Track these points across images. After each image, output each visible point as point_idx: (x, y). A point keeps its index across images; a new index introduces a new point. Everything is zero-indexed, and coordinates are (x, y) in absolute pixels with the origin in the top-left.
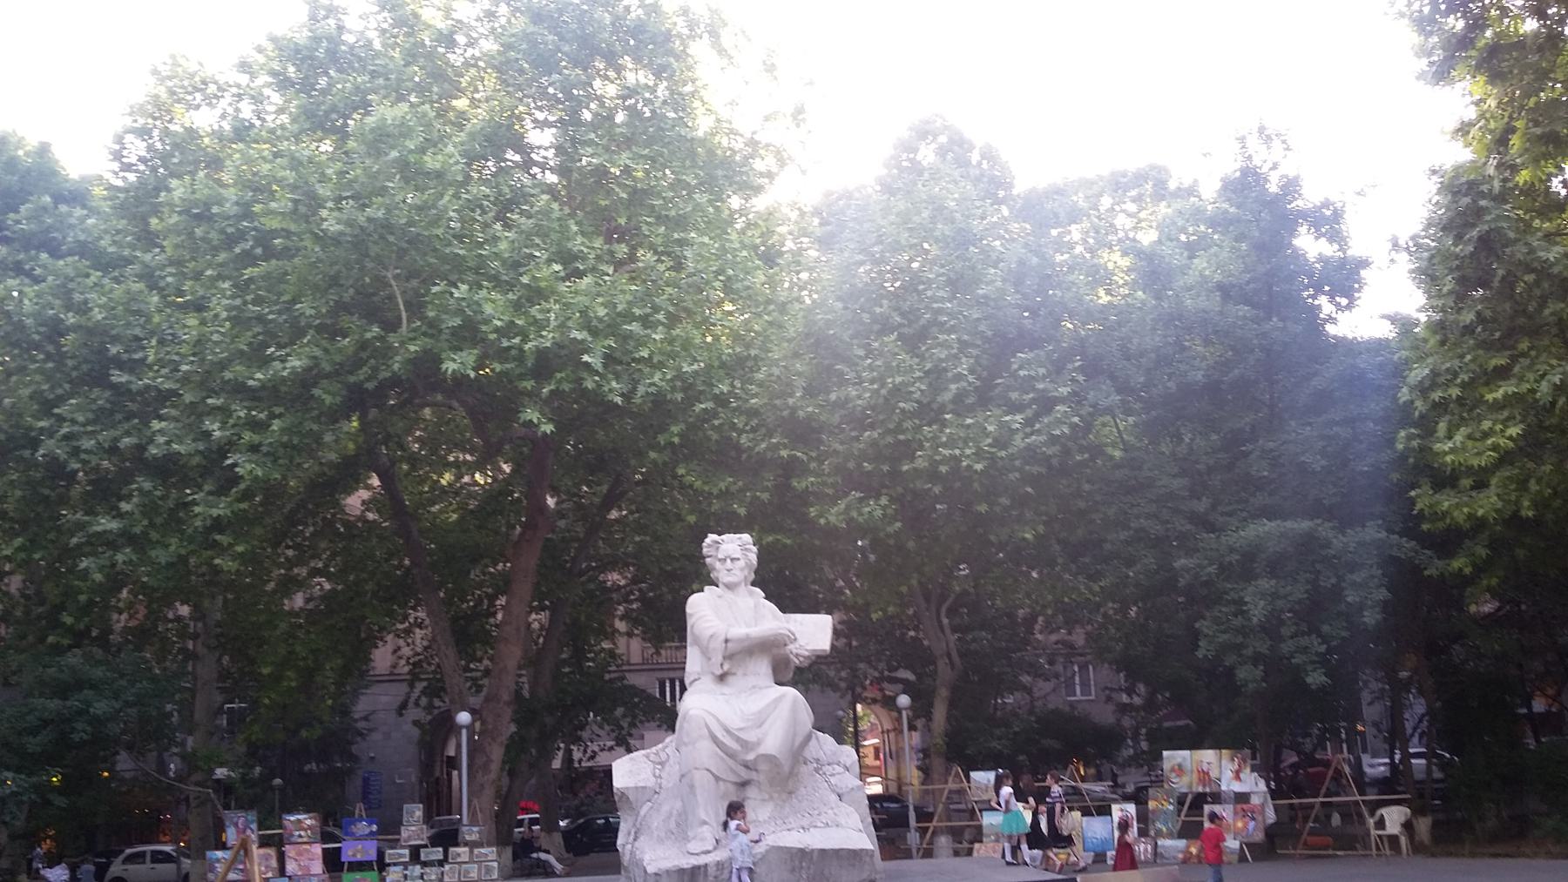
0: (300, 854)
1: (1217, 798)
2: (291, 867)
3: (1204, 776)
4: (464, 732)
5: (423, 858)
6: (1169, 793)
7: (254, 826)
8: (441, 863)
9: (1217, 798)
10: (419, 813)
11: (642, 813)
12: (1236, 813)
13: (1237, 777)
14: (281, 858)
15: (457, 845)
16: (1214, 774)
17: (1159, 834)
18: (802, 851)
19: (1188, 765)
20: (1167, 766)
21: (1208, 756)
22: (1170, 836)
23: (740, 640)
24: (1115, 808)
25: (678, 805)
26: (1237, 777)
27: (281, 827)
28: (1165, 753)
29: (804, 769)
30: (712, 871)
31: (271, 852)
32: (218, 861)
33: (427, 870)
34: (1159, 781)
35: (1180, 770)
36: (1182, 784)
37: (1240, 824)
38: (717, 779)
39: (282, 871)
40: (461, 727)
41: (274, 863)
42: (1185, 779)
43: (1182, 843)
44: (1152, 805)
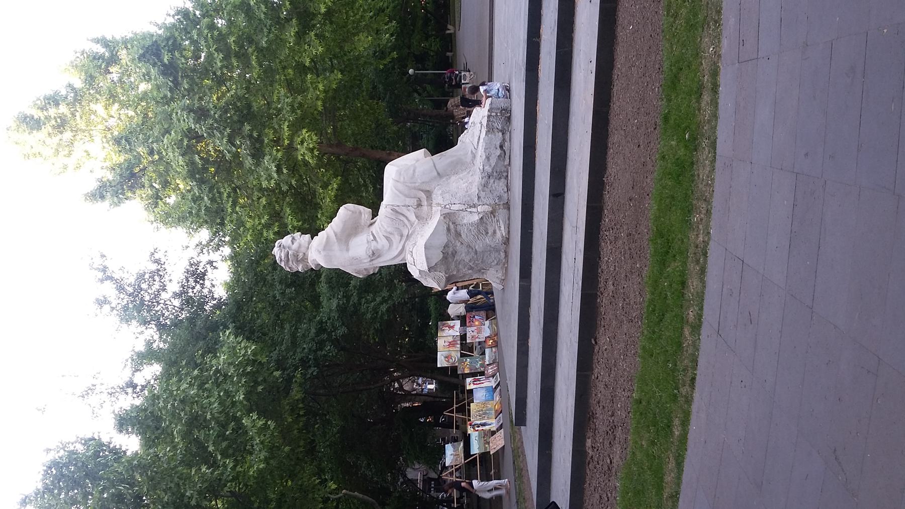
1: (463, 337)
3: (451, 344)
6: (460, 362)
9: (463, 337)
11: (455, 208)
12: (471, 326)
13: (453, 327)
16: (451, 339)
17: (482, 366)
19: (446, 353)
20: (445, 365)
21: (441, 343)
22: (484, 359)
24: (468, 388)
25: (453, 178)
26: (453, 327)
28: (439, 366)
34: (454, 369)
35: (448, 357)
36: (456, 354)
37: (477, 323)
42: (453, 354)
43: (487, 351)
44: (467, 371)
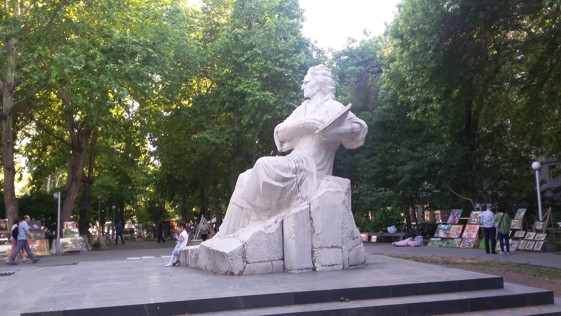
0: (470, 229)
2: (465, 234)
4: (537, 172)
5: (515, 236)
7: (459, 216)
8: (523, 238)
10: (523, 214)
14: (463, 231)
15: (532, 231)
18: (208, 248)
23: (282, 131)
27: (468, 215)
29: (295, 203)
30: (189, 253)
31: (461, 227)
32: (441, 229)
33: (514, 242)
38: (242, 208)
39: (461, 236)
40: (535, 171)
41: (460, 232)
